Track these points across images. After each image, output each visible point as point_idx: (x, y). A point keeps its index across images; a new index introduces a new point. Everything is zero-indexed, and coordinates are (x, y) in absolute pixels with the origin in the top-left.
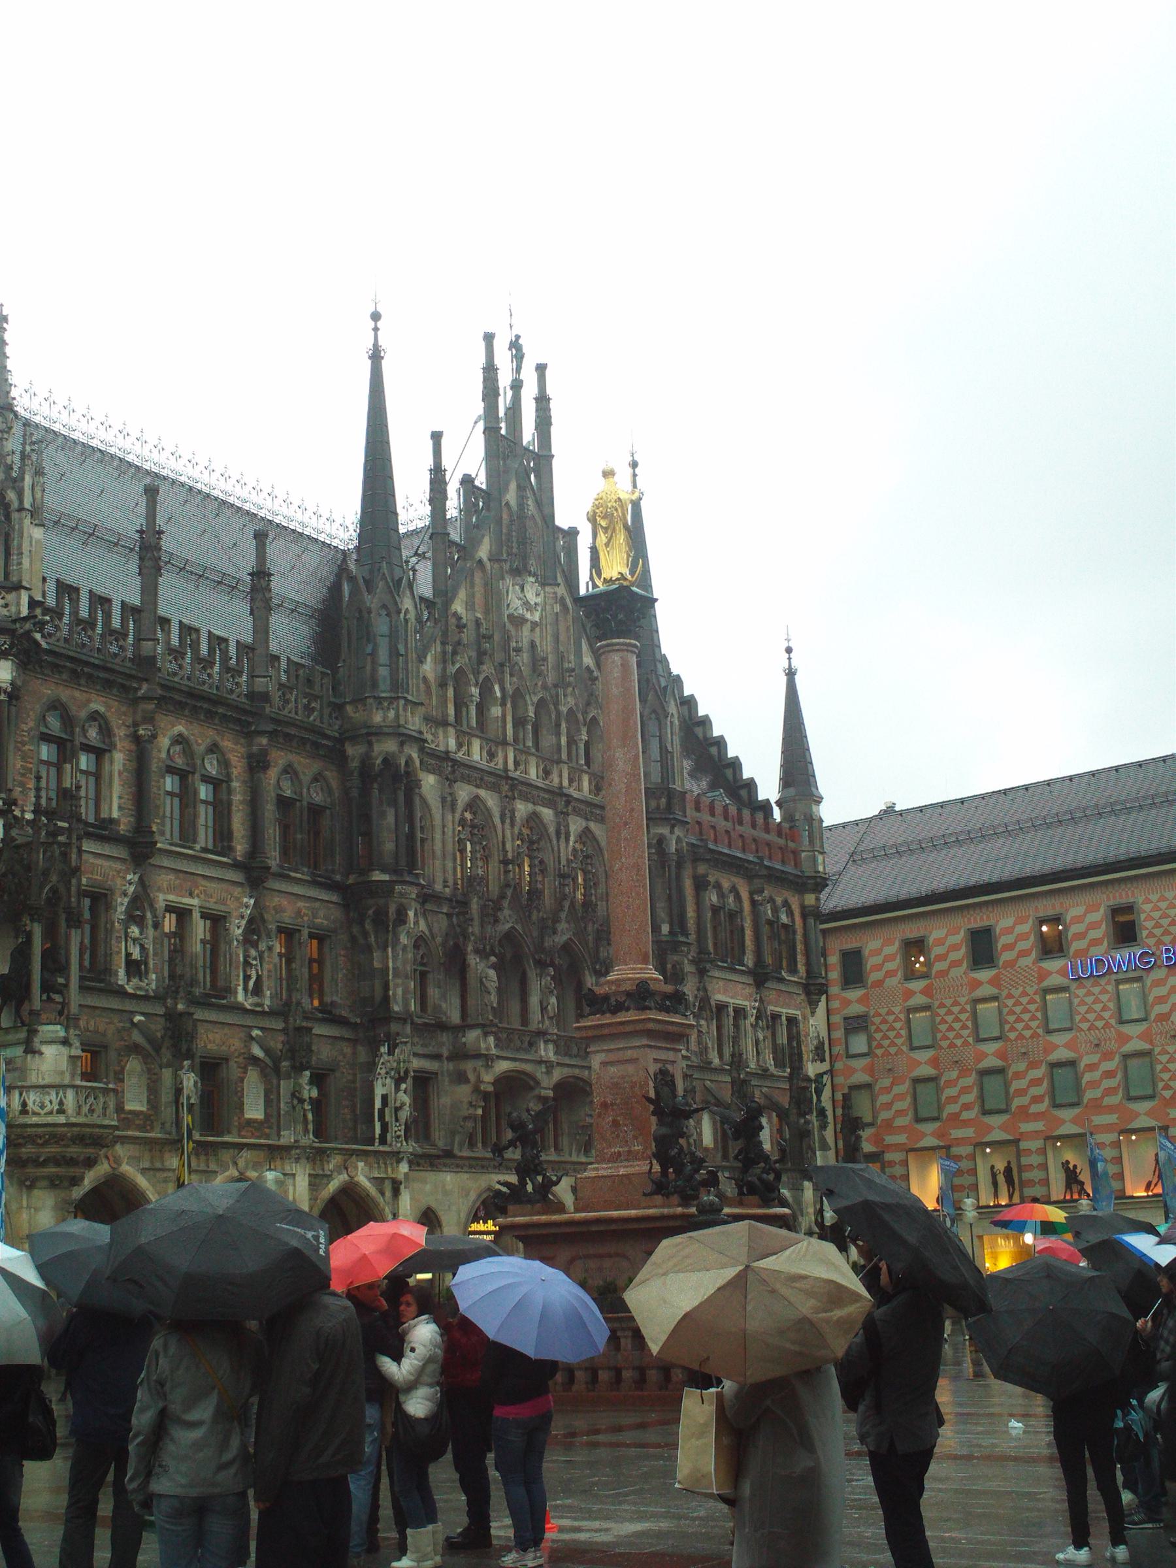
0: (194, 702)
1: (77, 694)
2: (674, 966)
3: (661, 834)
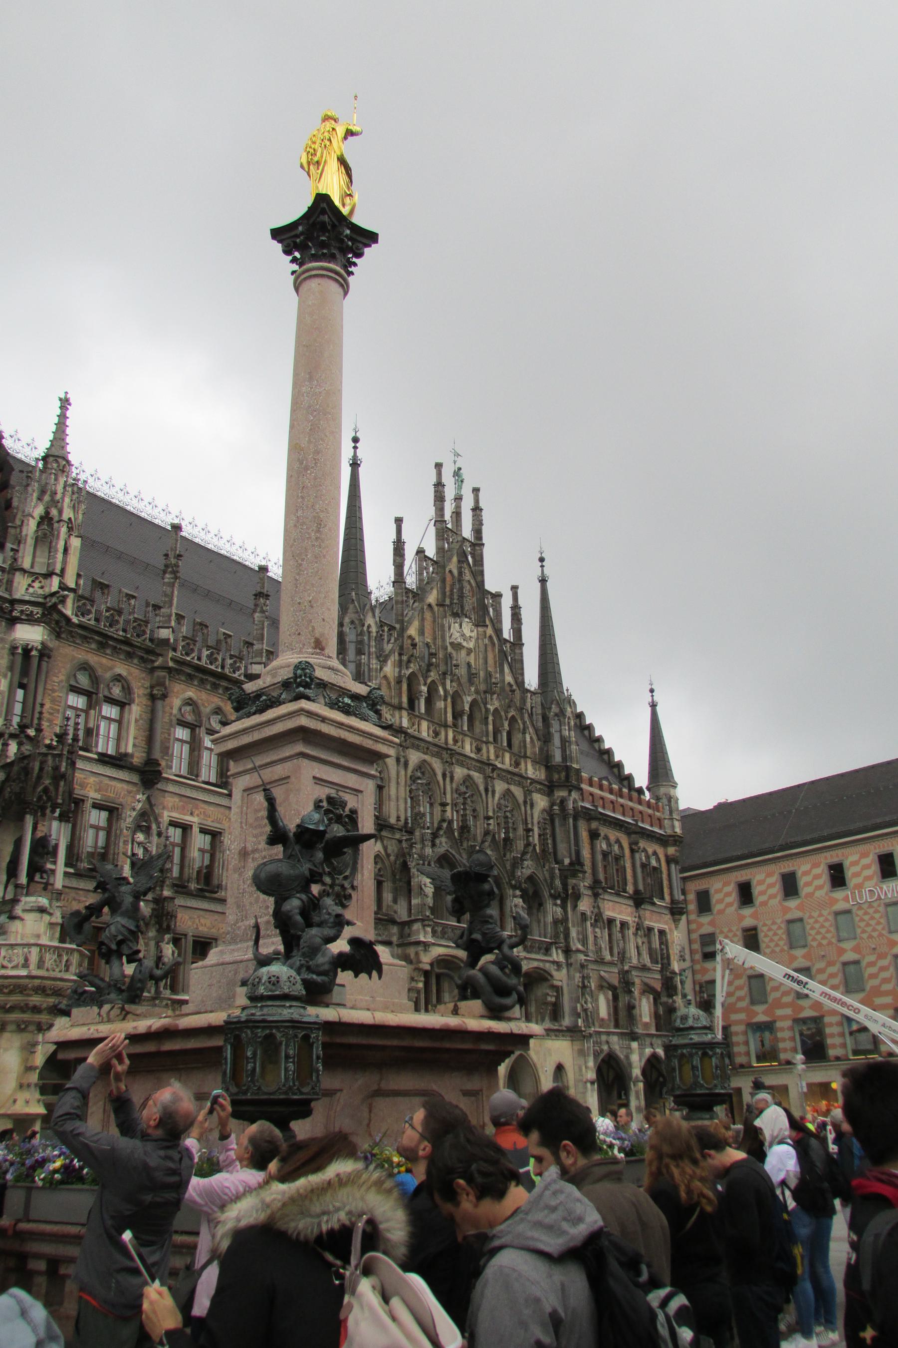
0: (201, 675)
1: (104, 661)
2: (573, 888)
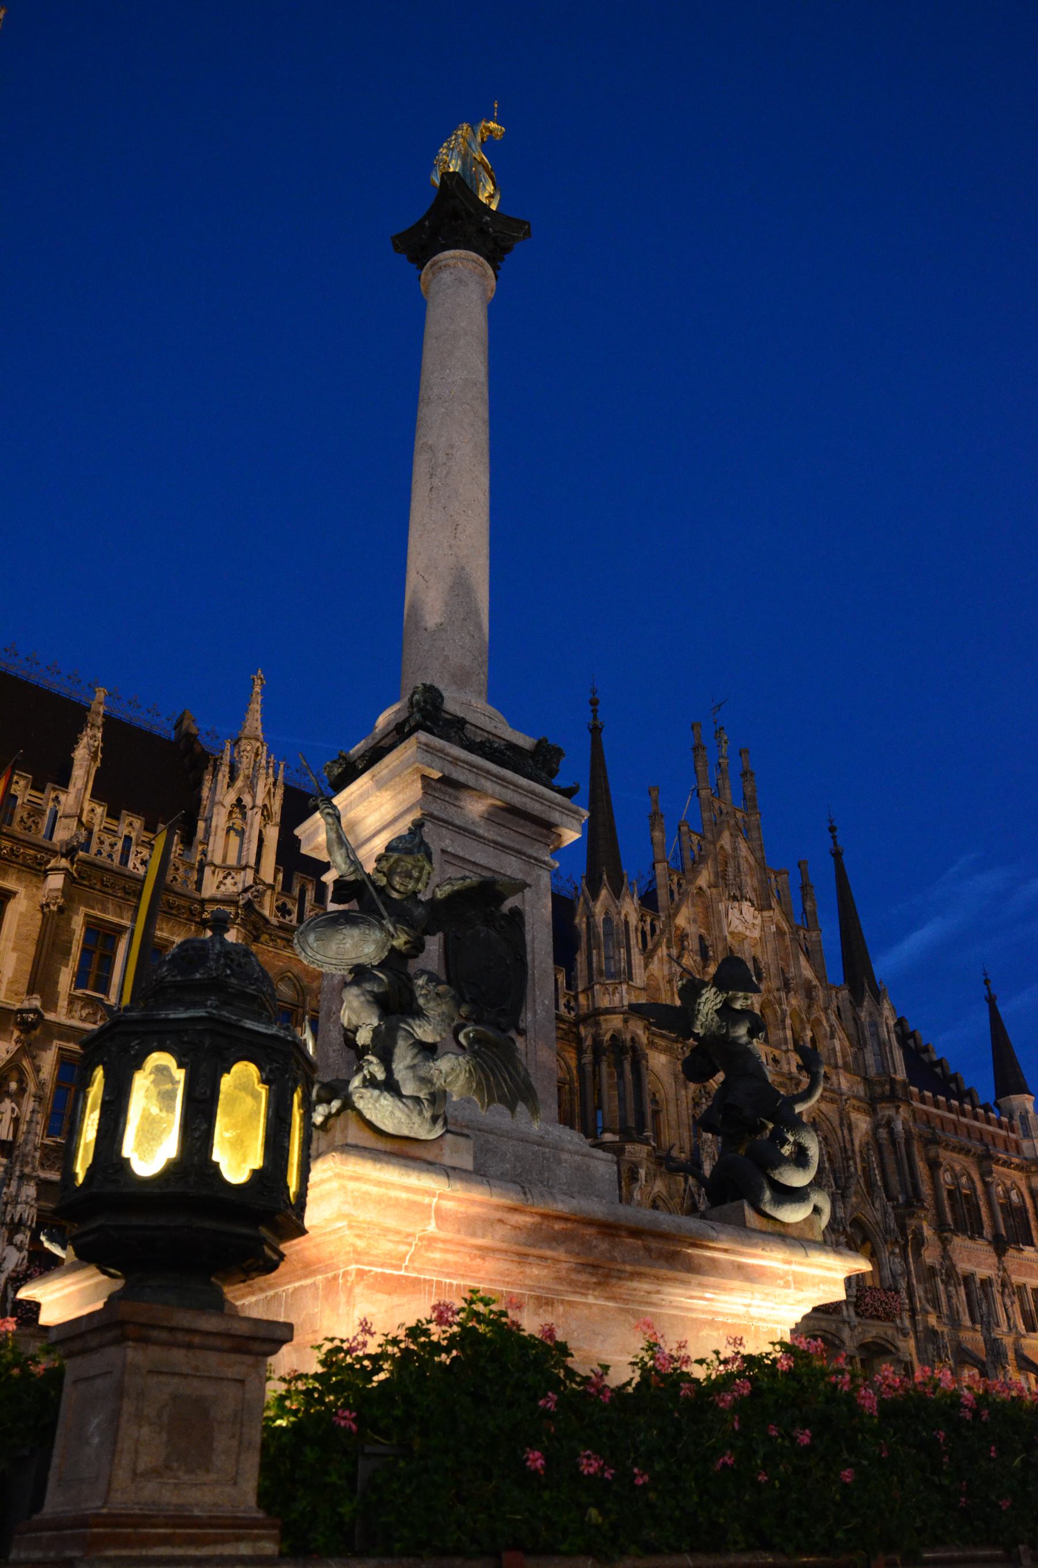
3: (889, 1115)
